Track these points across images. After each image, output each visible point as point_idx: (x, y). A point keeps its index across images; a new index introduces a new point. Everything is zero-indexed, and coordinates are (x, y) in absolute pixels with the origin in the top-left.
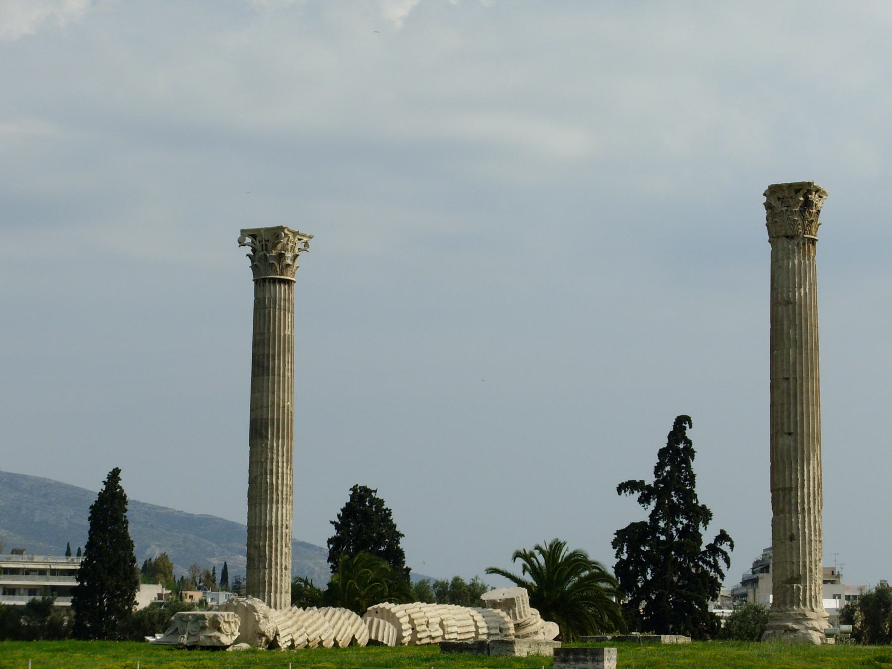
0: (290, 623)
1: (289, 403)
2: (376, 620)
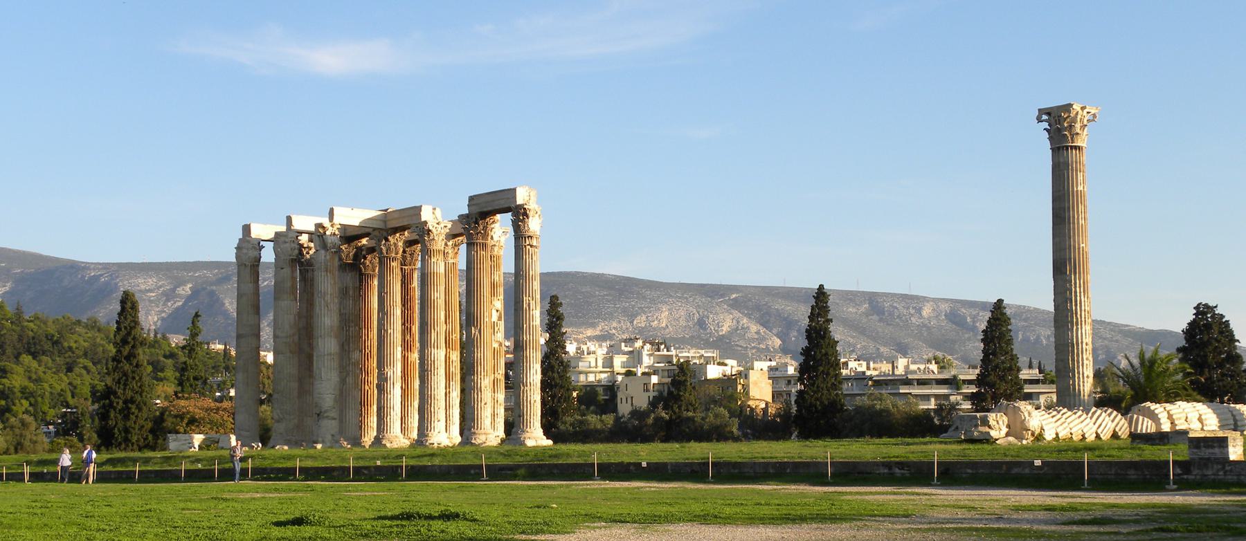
0: (1055, 419)
1: (1084, 245)
2: (1135, 416)
